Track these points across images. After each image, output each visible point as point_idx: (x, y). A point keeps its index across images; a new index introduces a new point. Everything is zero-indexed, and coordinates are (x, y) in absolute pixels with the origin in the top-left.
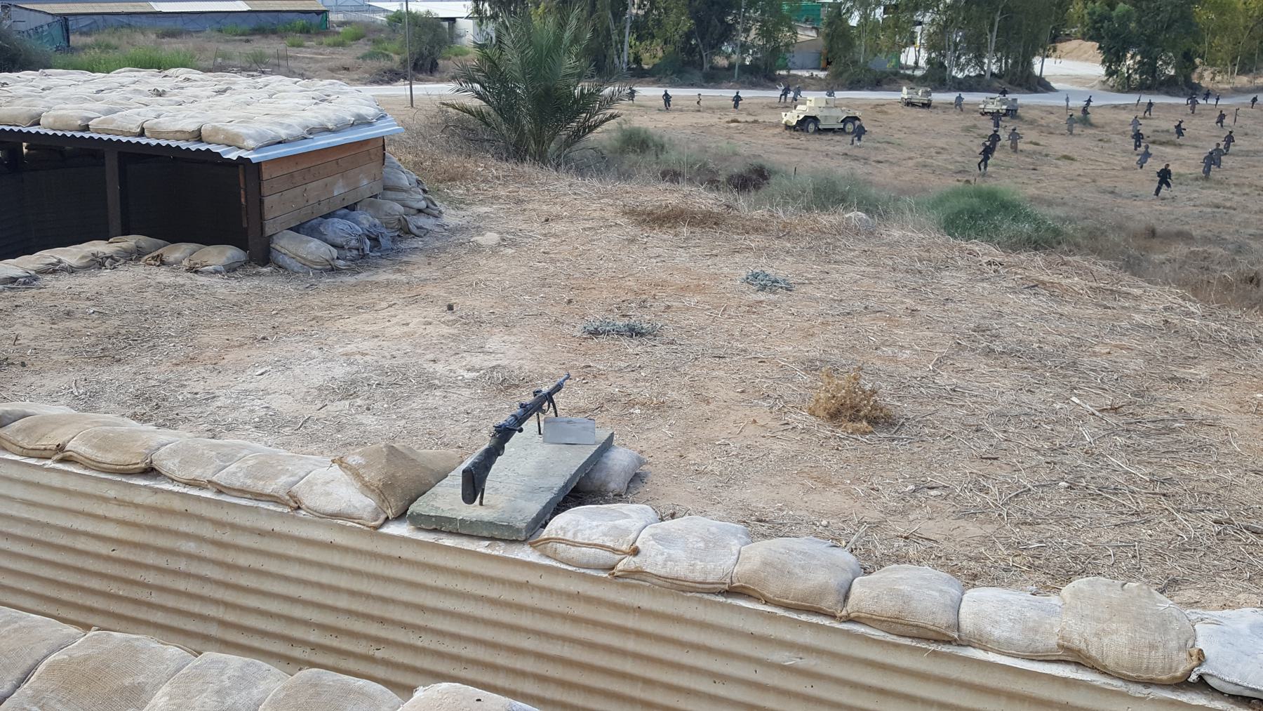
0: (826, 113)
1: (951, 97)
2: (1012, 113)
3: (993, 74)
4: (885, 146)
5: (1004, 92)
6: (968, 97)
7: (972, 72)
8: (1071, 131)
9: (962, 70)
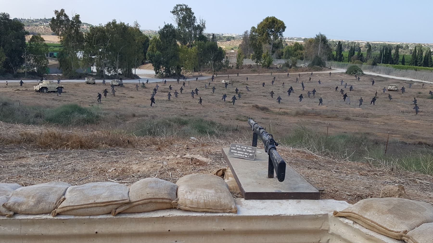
0: (50, 86)
1: (101, 81)
2: (121, 85)
3: (119, 74)
4: (70, 96)
6: (107, 81)
7: (112, 73)
8: (138, 90)
9: (110, 73)
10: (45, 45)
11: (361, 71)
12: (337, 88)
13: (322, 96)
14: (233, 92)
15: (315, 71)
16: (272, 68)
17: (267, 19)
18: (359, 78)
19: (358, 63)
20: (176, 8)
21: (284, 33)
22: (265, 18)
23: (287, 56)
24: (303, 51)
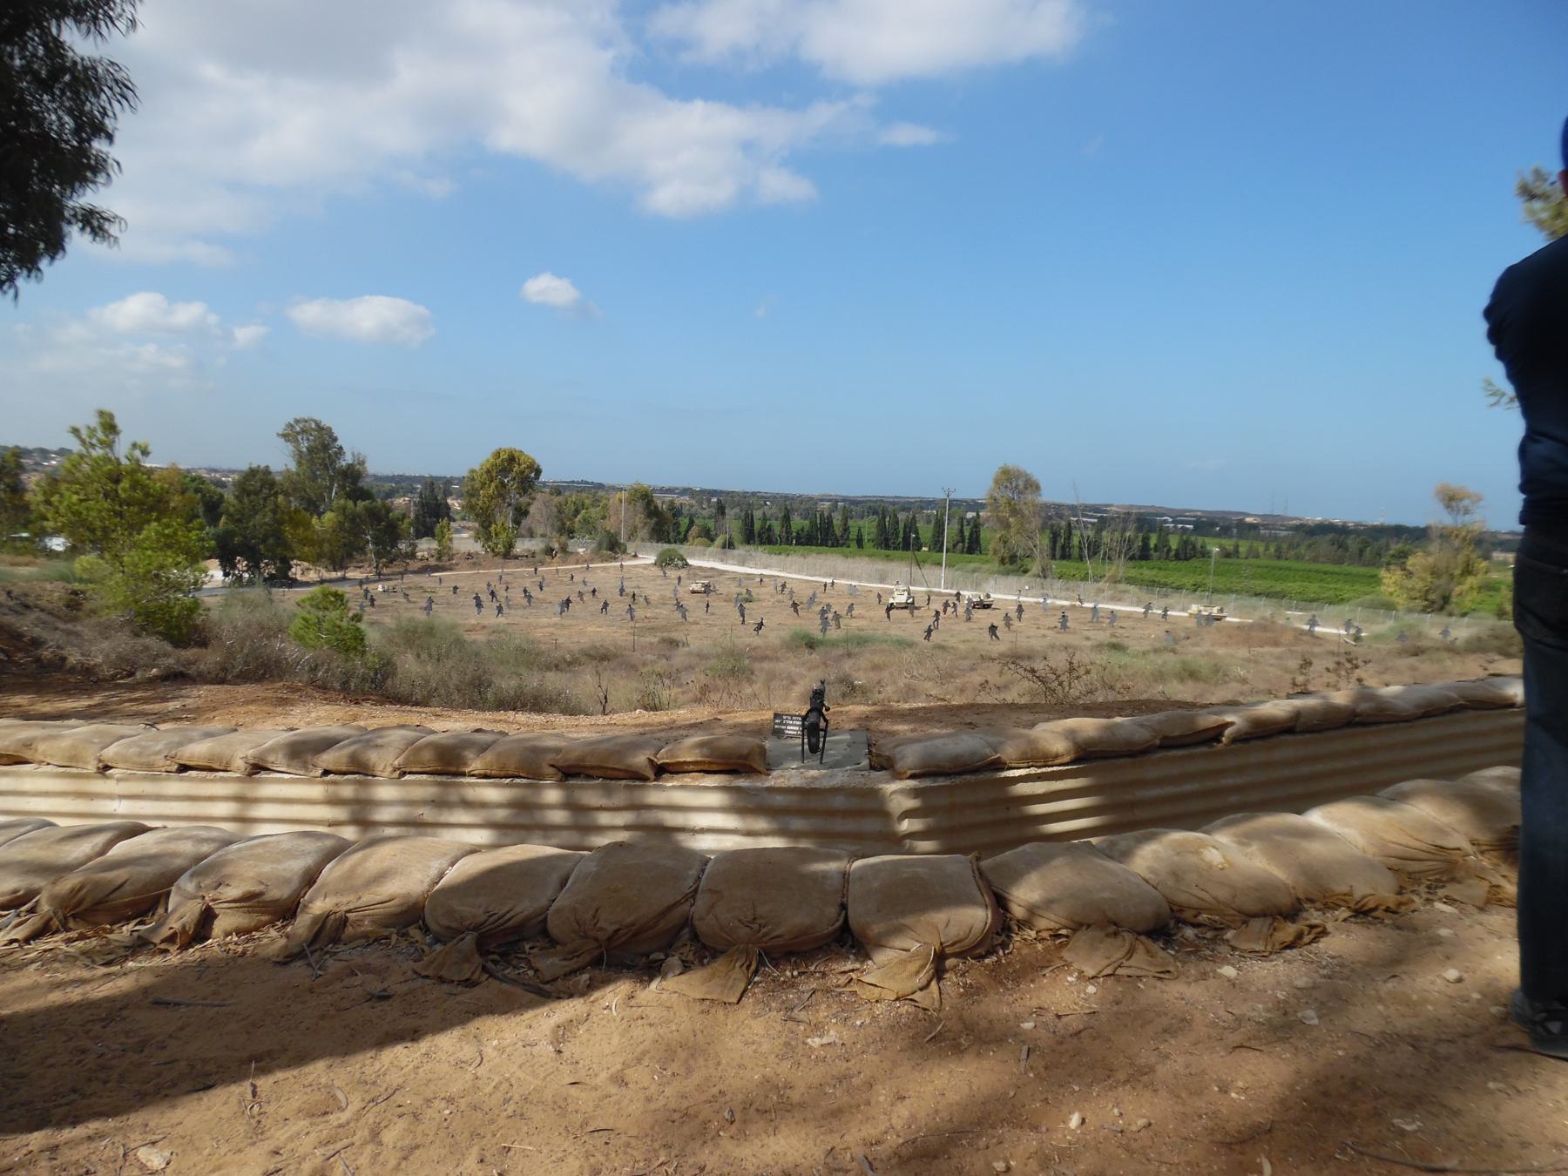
16: (516, 557)
22: (494, 449)
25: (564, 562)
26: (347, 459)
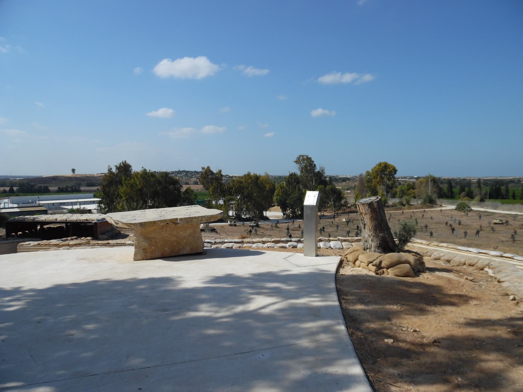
5: (256, 221)
10: (196, 195)
11: (469, 207)
12: (447, 223)
13: (433, 231)
14: (354, 229)
15: (427, 208)
17: (380, 164)
18: (467, 214)
19: (467, 200)
20: (299, 158)
21: (396, 176)
22: (378, 163)
23: (401, 195)
24: (415, 190)
25: (410, 209)
26: (317, 169)
